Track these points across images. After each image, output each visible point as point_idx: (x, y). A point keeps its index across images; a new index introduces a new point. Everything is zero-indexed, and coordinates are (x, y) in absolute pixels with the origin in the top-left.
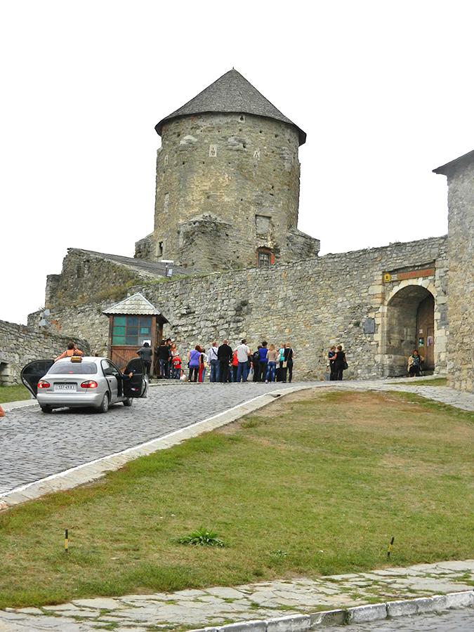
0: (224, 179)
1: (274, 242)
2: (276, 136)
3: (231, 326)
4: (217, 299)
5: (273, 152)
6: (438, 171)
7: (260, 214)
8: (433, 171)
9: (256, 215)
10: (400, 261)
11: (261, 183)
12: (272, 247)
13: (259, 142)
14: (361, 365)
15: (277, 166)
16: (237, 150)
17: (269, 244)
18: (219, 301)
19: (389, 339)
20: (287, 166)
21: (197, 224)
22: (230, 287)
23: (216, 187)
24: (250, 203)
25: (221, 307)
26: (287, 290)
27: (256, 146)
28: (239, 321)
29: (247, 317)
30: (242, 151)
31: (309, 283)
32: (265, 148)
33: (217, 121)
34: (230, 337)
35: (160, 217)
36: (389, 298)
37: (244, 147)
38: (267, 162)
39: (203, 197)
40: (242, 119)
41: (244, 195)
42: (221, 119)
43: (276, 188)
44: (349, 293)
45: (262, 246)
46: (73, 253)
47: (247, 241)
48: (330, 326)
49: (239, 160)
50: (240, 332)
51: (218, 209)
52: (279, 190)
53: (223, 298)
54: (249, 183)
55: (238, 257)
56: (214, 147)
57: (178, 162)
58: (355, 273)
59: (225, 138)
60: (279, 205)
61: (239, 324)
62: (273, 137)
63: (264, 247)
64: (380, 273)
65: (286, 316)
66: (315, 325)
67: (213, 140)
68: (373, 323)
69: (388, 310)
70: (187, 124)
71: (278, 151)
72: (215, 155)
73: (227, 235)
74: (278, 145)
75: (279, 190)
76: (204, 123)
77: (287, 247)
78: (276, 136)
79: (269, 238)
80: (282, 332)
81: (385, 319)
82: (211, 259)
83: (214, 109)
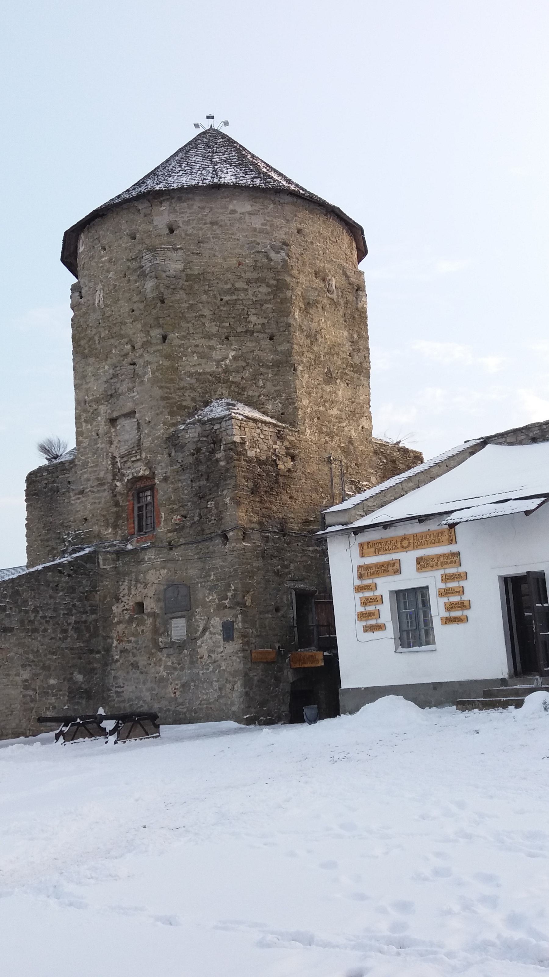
7: (115, 415)
12: (147, 473)
15: (136, 298)
24: (97, 401)
32: (111, 275)
54: (91, 360)
55: (86, 519)
62: (125, 242)
82: (47, 540)
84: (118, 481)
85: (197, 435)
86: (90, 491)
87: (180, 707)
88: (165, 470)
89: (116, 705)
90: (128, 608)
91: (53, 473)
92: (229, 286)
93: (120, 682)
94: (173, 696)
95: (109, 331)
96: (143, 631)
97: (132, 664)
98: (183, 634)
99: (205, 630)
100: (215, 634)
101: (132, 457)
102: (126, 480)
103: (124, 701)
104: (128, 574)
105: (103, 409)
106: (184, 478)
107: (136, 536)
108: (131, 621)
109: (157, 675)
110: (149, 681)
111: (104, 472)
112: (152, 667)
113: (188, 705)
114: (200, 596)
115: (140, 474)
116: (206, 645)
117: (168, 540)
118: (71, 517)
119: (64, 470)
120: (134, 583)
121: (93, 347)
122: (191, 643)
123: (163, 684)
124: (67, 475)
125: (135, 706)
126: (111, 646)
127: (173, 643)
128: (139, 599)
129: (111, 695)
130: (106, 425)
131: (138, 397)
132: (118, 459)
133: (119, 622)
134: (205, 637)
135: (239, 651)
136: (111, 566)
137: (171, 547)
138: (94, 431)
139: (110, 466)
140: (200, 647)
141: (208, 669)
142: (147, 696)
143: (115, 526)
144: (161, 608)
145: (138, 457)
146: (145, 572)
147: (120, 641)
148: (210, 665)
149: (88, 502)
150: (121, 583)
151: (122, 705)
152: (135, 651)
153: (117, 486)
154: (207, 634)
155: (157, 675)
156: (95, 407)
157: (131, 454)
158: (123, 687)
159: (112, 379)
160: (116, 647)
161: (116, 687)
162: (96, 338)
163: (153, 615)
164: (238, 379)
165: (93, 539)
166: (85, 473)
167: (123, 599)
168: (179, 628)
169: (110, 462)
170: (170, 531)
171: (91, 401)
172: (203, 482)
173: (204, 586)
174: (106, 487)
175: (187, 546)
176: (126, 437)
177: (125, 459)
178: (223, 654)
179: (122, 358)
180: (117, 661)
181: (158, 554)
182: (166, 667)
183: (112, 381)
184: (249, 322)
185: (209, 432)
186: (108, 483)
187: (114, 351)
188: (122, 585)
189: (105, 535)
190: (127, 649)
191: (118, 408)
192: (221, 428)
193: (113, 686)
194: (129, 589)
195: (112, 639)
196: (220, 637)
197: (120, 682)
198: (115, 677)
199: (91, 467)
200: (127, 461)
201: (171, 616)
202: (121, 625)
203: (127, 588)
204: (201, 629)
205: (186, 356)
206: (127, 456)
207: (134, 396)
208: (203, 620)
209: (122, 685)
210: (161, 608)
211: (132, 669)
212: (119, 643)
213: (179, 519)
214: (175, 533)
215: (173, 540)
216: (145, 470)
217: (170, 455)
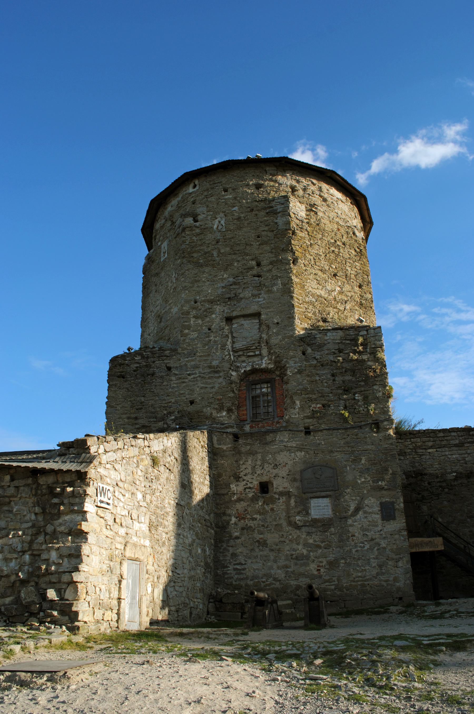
2: (258, 186)
7: (235, 314)
11: (232, 264)
17: (265, 363)
24: (211, 302)
30: (191, 228)
32: (236, 209)
37: (196, 221)
38: (240, 228)
40: (195, 187)
41: (199, 293)
43: (264, 263)
45: (248, 368)
47: (210, 367)
51: (167, 331)
52: (271, 263)
54: (207, 269)
55: (192, 402)
60: (275, 289)
63: (254, 371)
72: (166, 255)
73: (169, 369)
75: (271, 263)
77: (303, 357)
78: (258, 186)
79: (265, 352)
82: (136, 418)
84: (233, 370)
85: (339, 338)
86: (200, 376)
87: (327, 584)
88: (300, 365)
89: (234, 583)
90: (251, 486)
91: (148, 358)
92: (333, 241)
93: (241, 559)
94: (316, 573)
95: (231, 249)
96: (272, 509)
97: (258, 541)
98: (327, 513)
99: (357, 510)
100: (370, 513)
101: (249, 352)
102: (242, 371)
103: (247, 578)
104: (252, 453)
105: (218, 308)
106: (324, 372)
107: (248, 422)
108: (254, 499)
109: (294, 553)
110: (283, 558)
111: (217, 362)
112: (287, 545)
113: (336, 583)
114: (349, 477)
115: (262, 367)
116: (359, 524)
117: (306, 425)
118: (172, 398)
119: (162, 356)
120: (259, 463)
121: (210, 258)
122: (340, 521)
123: (302, 562)
124: (165, 361)
125: (262, 583)
126: (228, 522)
127: (315, 522)
128: (265, 479)
129: (228, 572)
130: (222, 322)
131: (264, 302)
132: (231, 353)
133: (239, 500)
134: (358, 517)
135: (403, 530)
136: (229, 446)
137: (308, 432)
138: (206, 326)
139: (227, 357)
140: (351, 526)
141: (364, 547)
142: (281, 574)
143: (229, 410)
144: (298, 488)
145: (257, 353)
146: (275, 453)
147: (240, 517)
148: (366, 543)
149: (196, 386)
150: (241, 463)
151: (243, 583)
152: (262, 529)
153: (232, 375)
154: (360, 513)
155: (294, 553)
157: (250, 349)
158: (245, 564)
159: (231, 285)
160: (235, 524)
161: (235, 564)
162: (215, 254)
163: (287, 494)
164: (342, 308)
165: (205, 420)
166: (193, 361)
167: (245, 478)
168: (321, 508)
169: (227, 353)
170: (308, 417)
171: (204, 301)
172: (348, 378)
173: (354, 469)
174: (221, 374)
175: (331, 432)
177: (241, 353)
178: (382, 532)
179: (244, 271)
180: (237, 538)
181: (293, 438)
182: (306, 545)
183: (231, 287)
184: (347, 270)
185: (353, 336)
186: (224, 371)
187: (236, 264)
188: (243, 464)
189: (218, 417)
190: (251, 527)
191: (239, 309)
192: (368, 334)
193: (230, 563)
194: (254, 468)
195: (230, 516)
196: (377, 517)
197: (241, 559)
198: (234, 555)
199: (201, 356)
200: (242, 355)
201: (311, 495)
202: (242, 502)
203: (250, 468)
204: (352, 508)
205: (310, 279)
206: (243, 350)
207: (260, 301)
208: (355, 500)
209: (244, 563)
210: (298, 488)
211: (259, 546)
212: (239, 520)
213: (319, 408)
214: (315, 420)
215: (313, 425)
216: (269, 363)
217: (304, 353)
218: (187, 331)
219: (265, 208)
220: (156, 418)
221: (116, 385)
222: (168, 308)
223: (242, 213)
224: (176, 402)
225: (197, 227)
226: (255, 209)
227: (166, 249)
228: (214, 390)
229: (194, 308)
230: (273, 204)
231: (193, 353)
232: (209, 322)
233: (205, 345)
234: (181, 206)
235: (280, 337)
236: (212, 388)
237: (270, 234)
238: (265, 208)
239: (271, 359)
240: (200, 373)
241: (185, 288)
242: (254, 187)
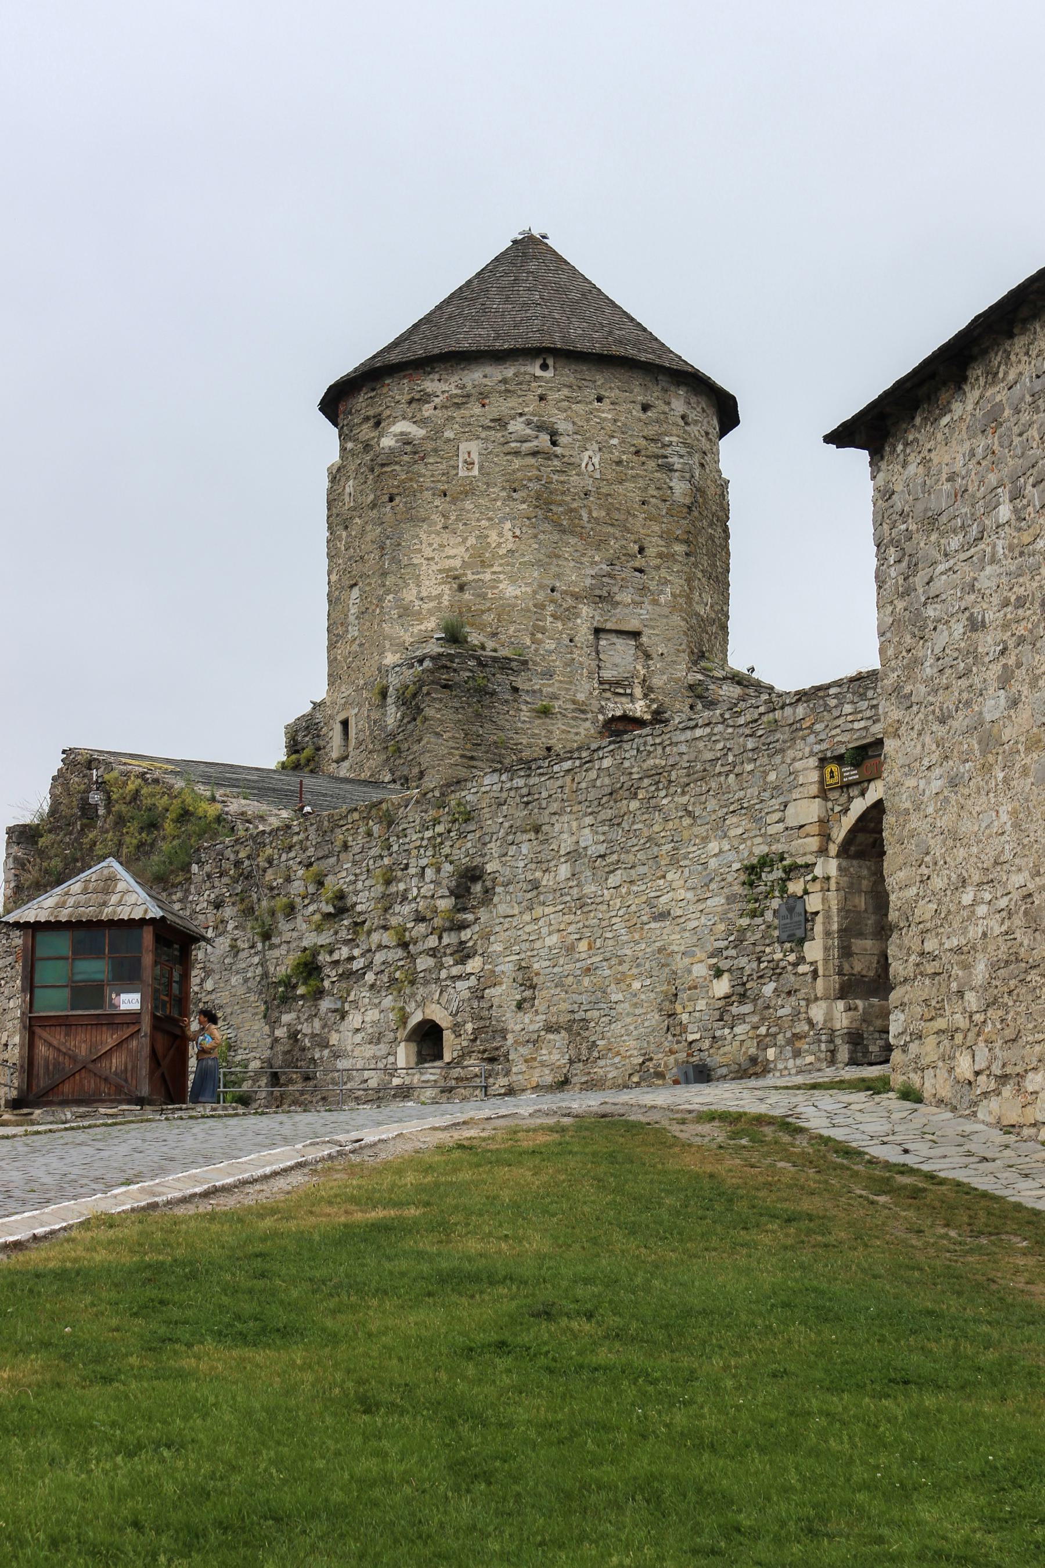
0: (500, 535)
1: (653, 701)
2: (645, 408)
3: (446, 940)
4: (407, 865)
5: (637, 453)
6: (842, 437)
8: (829, 439)
9: (597, 631)
10: (862, 724)
11: (605, 541)
13: (596, 427)
14: (775, 1035)
15: (652, 491)
16: (535, 454)
18: (412, 871)
19: (846, 952)
20: (680, 488)
21: (427, 663)
22: (440, 829)
23: (480, 560)
24: (576, 597)
25: (419, 889)
26: (581, 828)
27: (588, 439)
28: (463, 926)
29: (483, 914)
30: (549, 456)
31: (634, 805)
32: (615, 441)
33: (475, 377)
34: (444, 974)
35: (340, 652)
36: (839, 834)
37: (554, 443)
39: (446, 588)
40: (544, 367)
41: (558, 576)
42: (489, 370)
43: (651, 551)
44: (737, 826)
45: (619, 713)
46: (79, 764)
47: (574, 702)
48: (695, 924)
49: (539, 479)
50: (468, 957)
52: (660, 555)
53: (424, 862)
54: (573, 541)
56: (470, 449)
57: (377, 498)
58: (749, 767)
59: (501, 422)
60: (662, 599)
61: (465, 934)
62: (637, 412)
64: (813, 762)
65: (581, 903)
66: (653, 925)
67: (468, 430)
68: (799, 908)
69: (840, 868)
70: (398, 390)
71: (653, 448)
72: (475, 472)
73: (516, 690)
74: (651, 431)
75: (660, 555)
76: (440, 386)
78: (645, 408)
79: (638, 691)
80: (570, 949)
81: (834, 899)
82: (472, 758)
83: (465, 345)
91: (486, 666)
105: (585, 610)
145: (628, 691)
156: (570, 602)
166: (550, 686)
171: (565, 592)
174: (589, 716)
176: (618, 660)
177: (607, 687)
199: (561, 682)
217: (692, 707)
218: (539, 636)
219: (657, 457)
220: (501, 762)
221: (441, 700)
222: (488, 577)
223: (624, 452)
224: (530, 746)
225: (557, 456)
226: (643, 453)
227: (475, 457)
228: (577, 738)
229: (551, 601)
230: (668, 451)
231: (549, 674)
232: (572, 629)
233: (566, 665)
234: (514, 392)
235: (665, 677)
236: (577, 734)
237: (661, 505)
238: (657, 457)
239: (649, 707)
240: (560, 707)
241: (539, 563)
242: (639, 407)
